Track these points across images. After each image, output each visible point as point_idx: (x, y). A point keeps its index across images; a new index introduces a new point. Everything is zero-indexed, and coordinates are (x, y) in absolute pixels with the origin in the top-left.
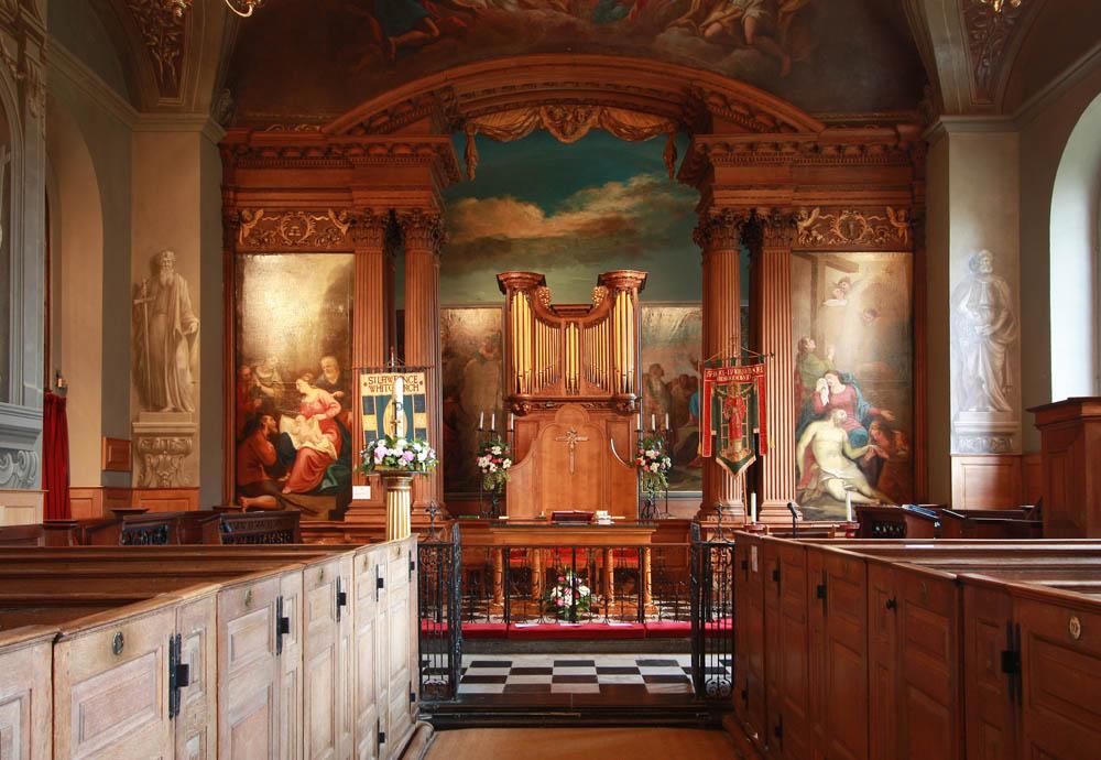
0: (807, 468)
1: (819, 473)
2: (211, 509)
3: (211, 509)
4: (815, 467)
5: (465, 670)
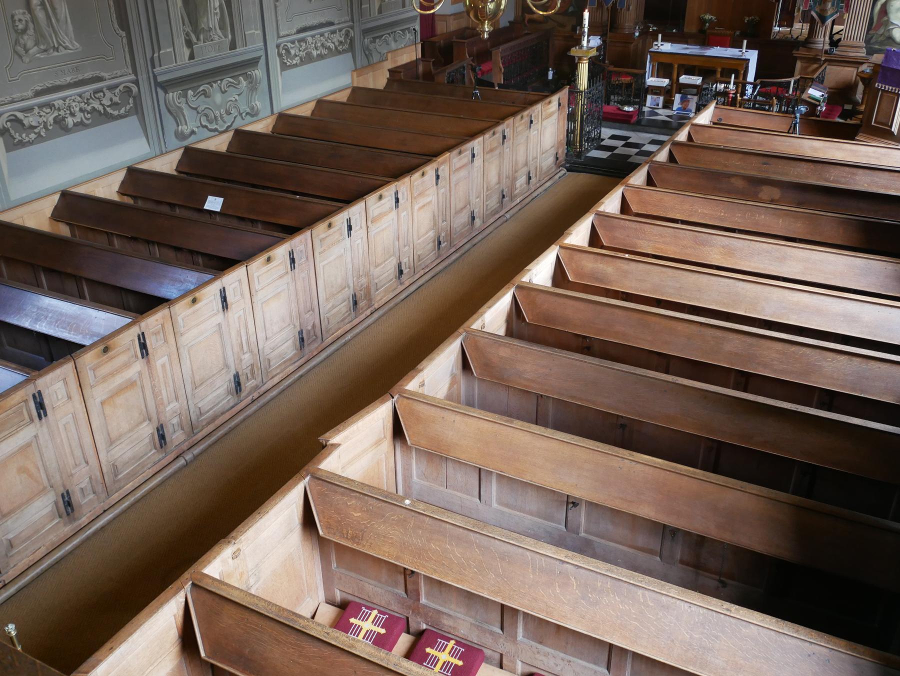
0: (880, 17)
1: (888, 23)
2: (508, 24)
3: (508, 24)
4: (885, 19)
5: (603, 140)
